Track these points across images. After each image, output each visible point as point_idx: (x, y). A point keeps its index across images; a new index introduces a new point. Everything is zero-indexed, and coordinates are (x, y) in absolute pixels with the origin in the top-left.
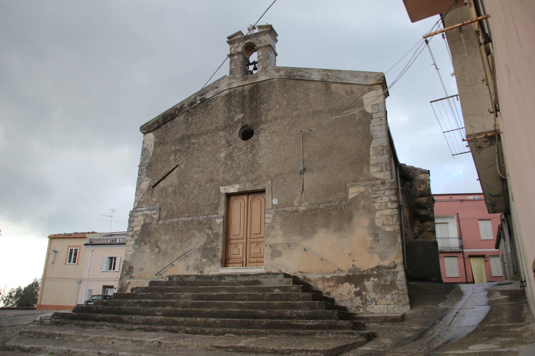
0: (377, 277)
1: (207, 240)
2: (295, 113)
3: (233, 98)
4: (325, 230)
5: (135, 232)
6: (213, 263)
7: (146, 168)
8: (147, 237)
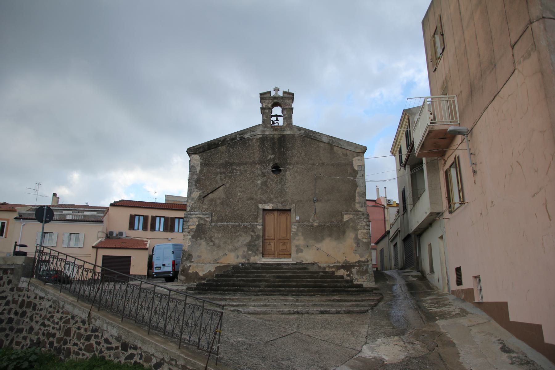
0: (358, 267)
2: (311, 162)
3: (266, 142)
4: (329, 238)
5: (191, 229)
6: (256, 254)
7: (195, 182)
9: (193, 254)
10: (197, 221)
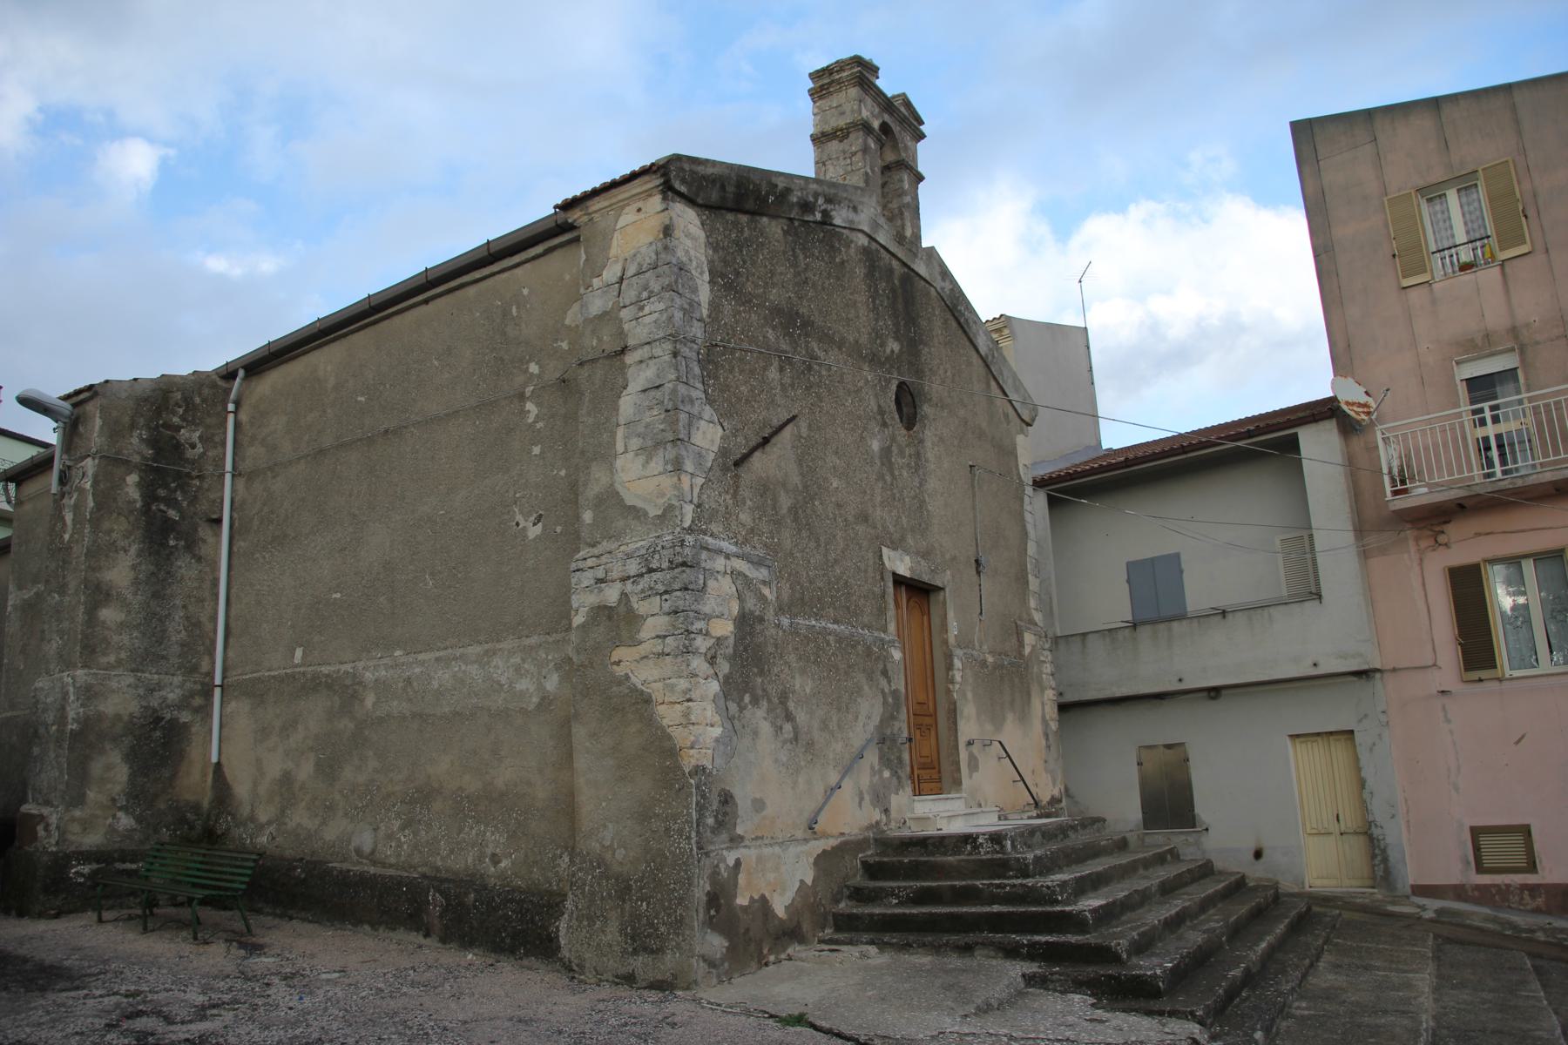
9: (738, 793)
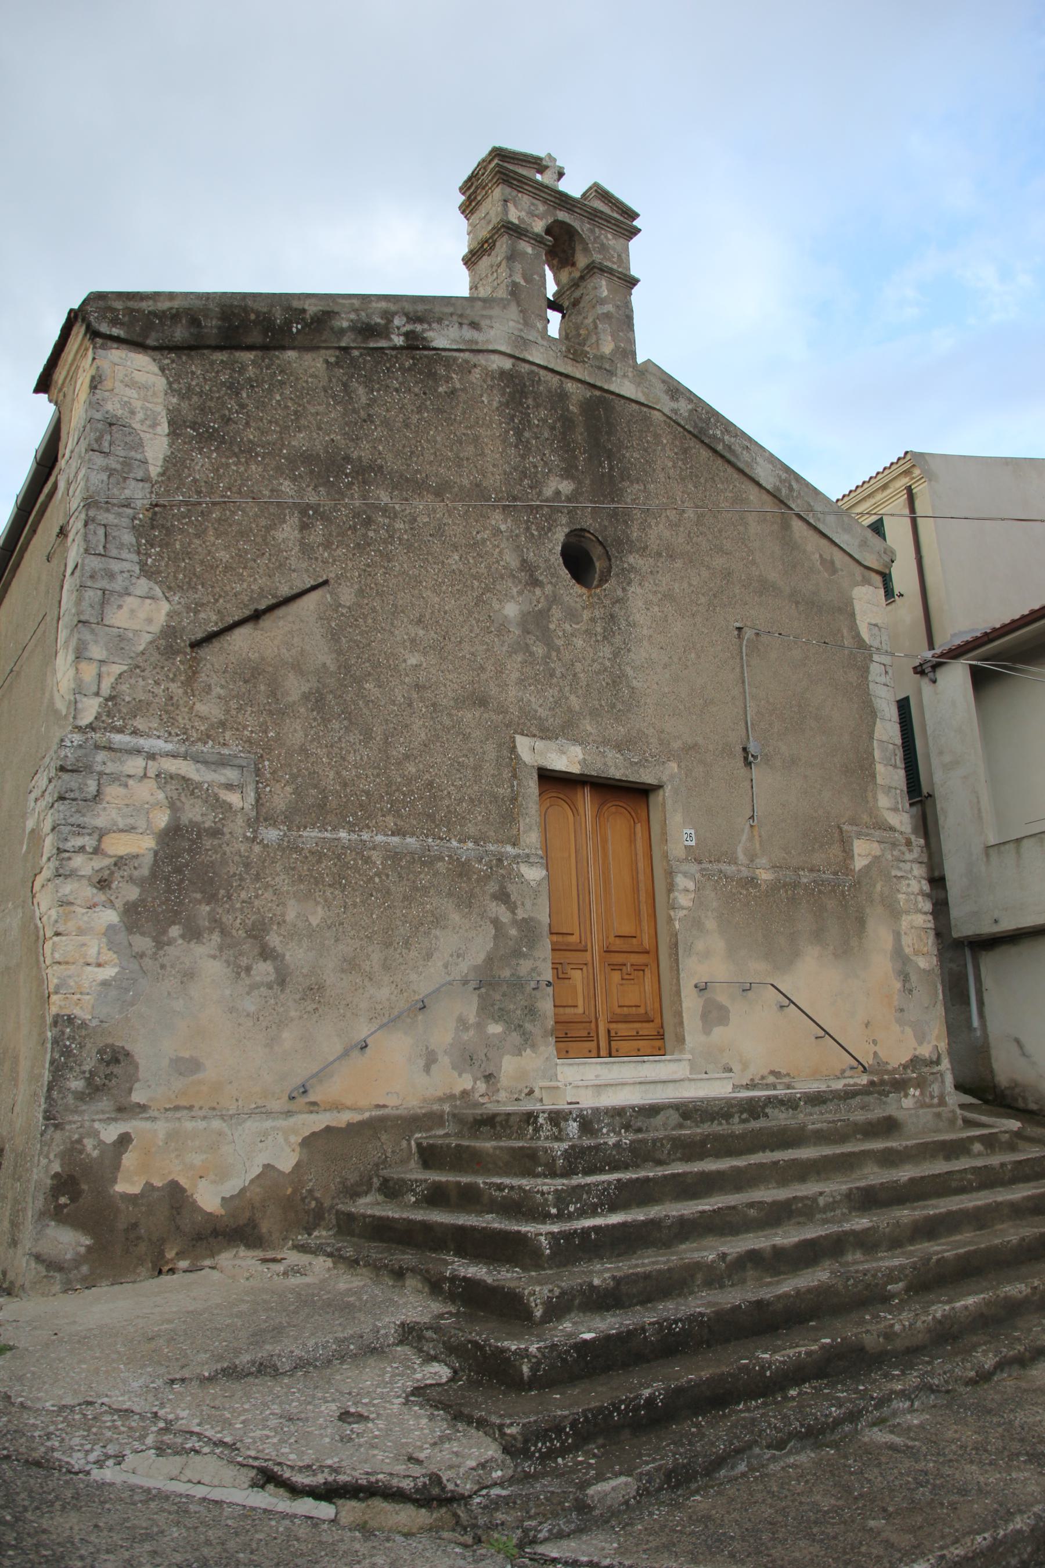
1: (495, 944)
2: (719, 562)
3: (530, 402)
5: (120, 862)
6: (528, 1040)
7: (137, 531)
8: (198, 896)
9: (140, 1050)
10: (157, 804)
